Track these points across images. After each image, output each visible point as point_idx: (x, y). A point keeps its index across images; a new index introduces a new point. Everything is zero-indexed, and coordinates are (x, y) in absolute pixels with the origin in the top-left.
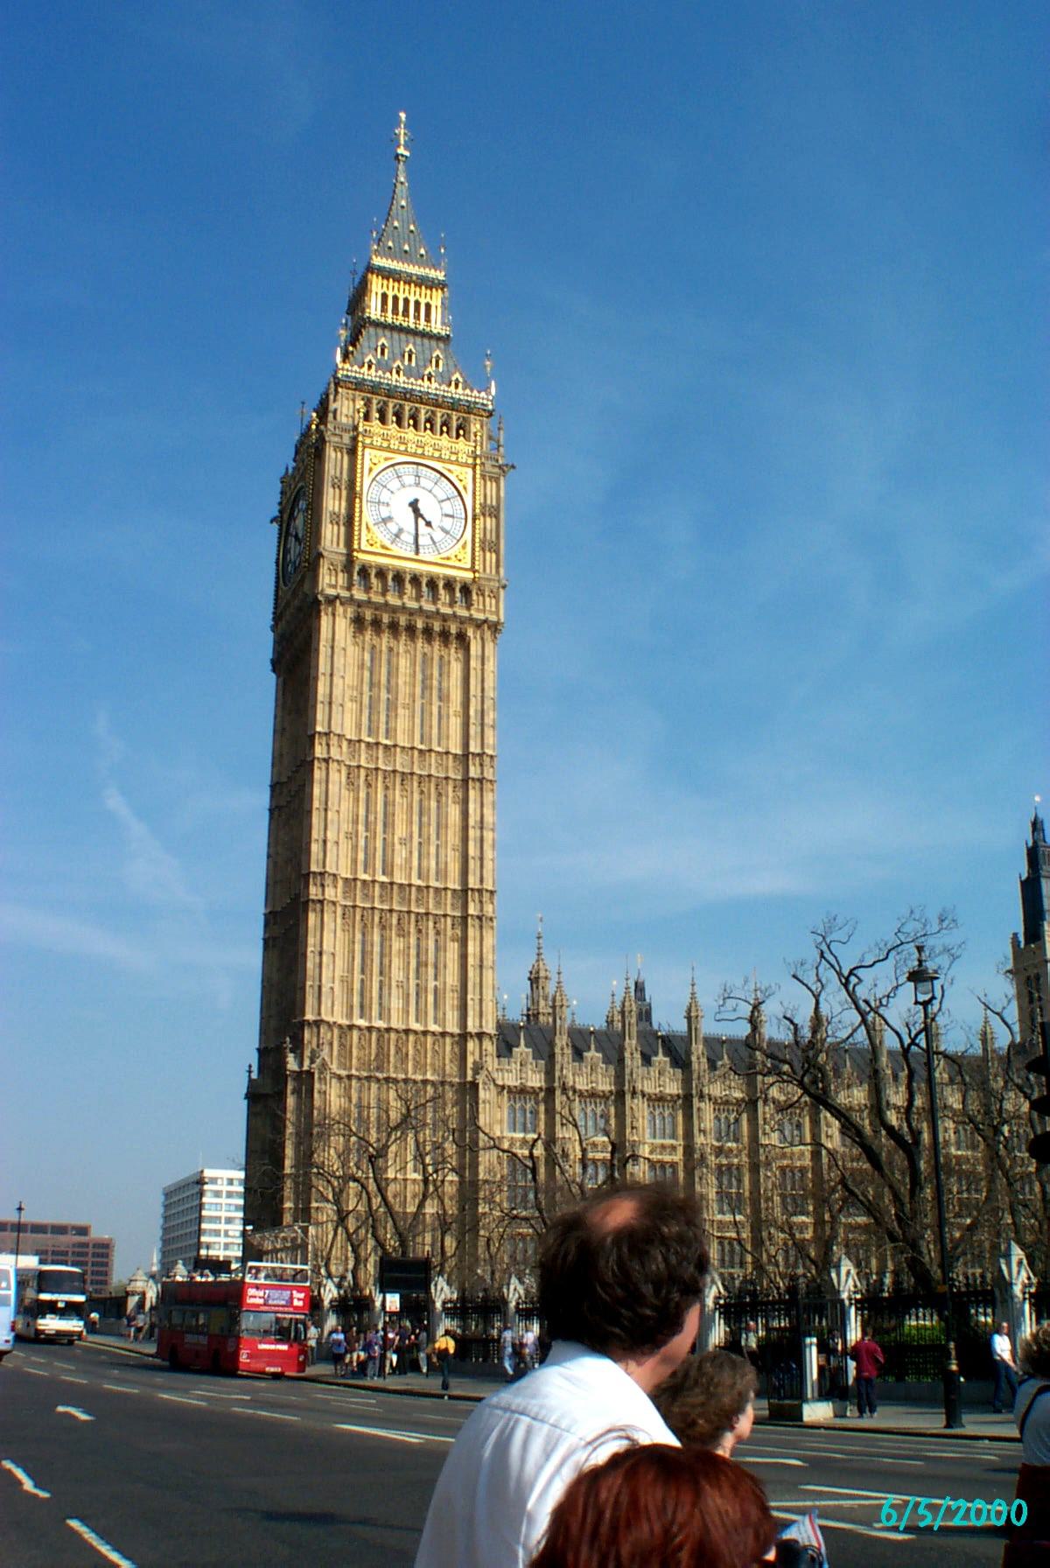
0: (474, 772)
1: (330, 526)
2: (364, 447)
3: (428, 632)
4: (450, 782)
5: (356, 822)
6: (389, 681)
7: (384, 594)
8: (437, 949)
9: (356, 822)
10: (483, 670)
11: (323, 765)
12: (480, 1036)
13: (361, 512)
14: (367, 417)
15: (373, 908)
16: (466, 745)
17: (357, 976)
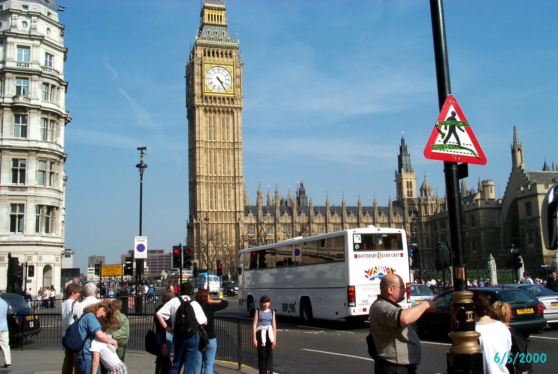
0: (236, 147)
1: (197, 86)
2: (204, 64)
3: (223, 111)
4: (231, 150)
5: (207, 162)
6: (214, 125)
7: (211, 103)
8: (229, 191)
9: (207, 162)
12: (240, 212)
13: (204, 82)
14: (205, 55)
15: (213, 183)
16: (234, 140)
17: (210, 199)
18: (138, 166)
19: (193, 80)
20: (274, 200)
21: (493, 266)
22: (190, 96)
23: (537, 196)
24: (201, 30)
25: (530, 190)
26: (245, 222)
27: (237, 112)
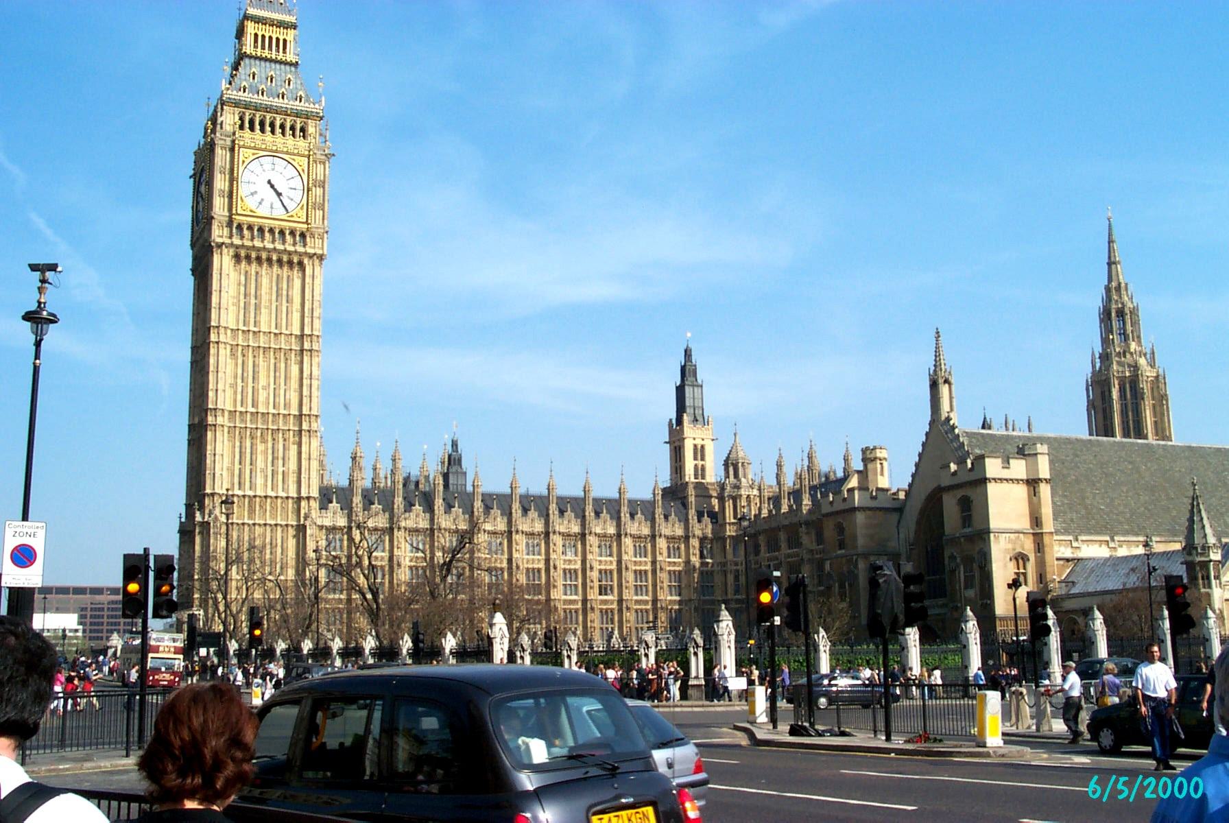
0: (307, 346)
1: (218, 198)
2: (239, 148)
3: (280, 261)
4: (293, 352)
6: (256, 292)
9: (236, 377)
10: (313, 284)
11: (216, 345)
12: (308, 498)
13: (237, 189)
15: (246, 427)
16: (302, 329)
17: (237, 466)
18: (28, 317)
19: (210, 184)
20: (389, 476)
21: (973, 635)
22: (202, 220)
23: (986, 483)
24: (236, 69)
25: (971, 470)
26: (320, 524)
27: (313, 265)
